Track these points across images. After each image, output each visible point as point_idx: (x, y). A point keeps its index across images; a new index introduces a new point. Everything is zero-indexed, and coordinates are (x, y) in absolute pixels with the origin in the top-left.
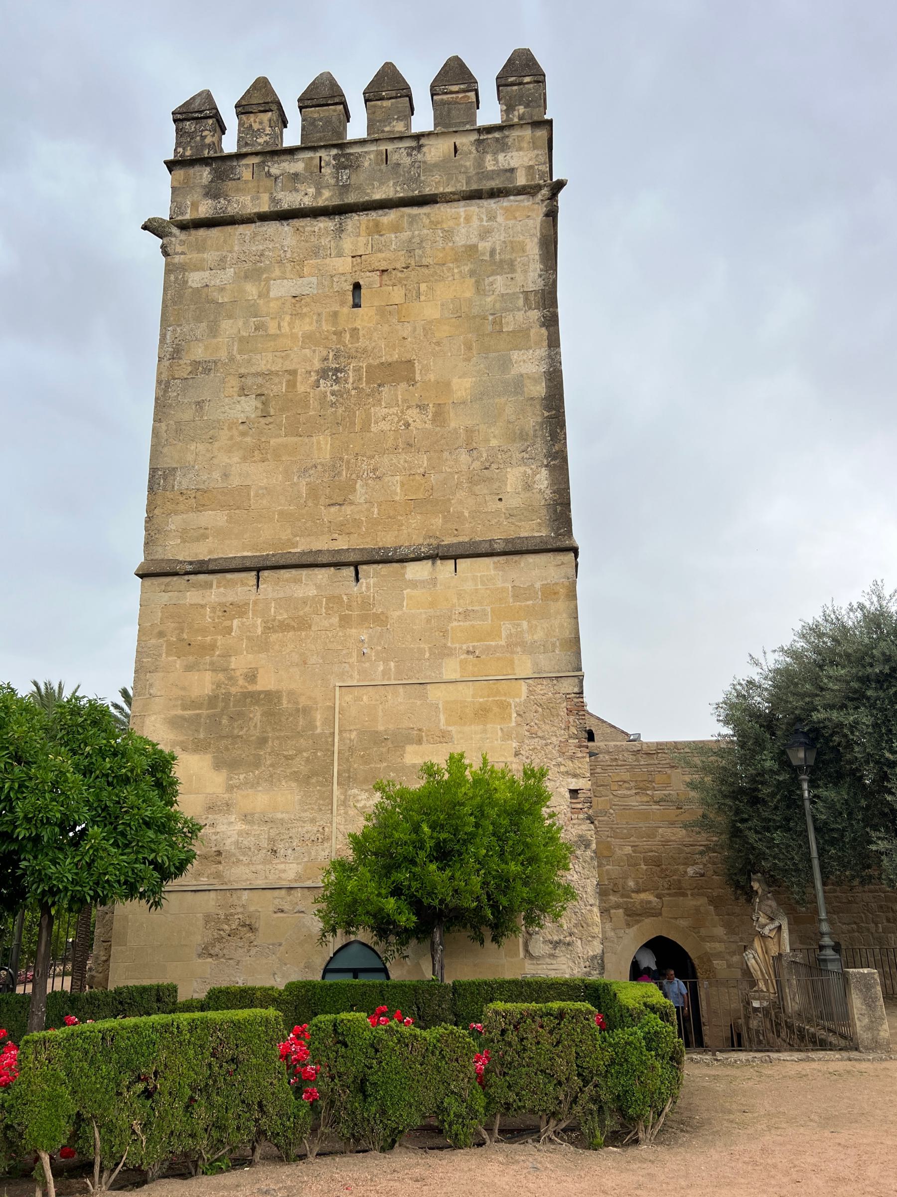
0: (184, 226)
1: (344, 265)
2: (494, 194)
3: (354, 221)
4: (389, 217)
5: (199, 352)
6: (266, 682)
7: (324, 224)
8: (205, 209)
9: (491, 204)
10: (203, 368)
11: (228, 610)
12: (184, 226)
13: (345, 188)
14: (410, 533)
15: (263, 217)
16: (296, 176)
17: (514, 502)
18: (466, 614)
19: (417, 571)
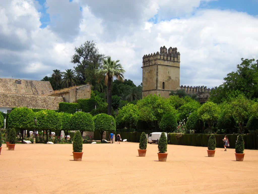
1: (149, 70)
7: (149, 67)
10: (144, 78)
13: (149, 64)
14: (151, 89)
16: (147, 63)
19: (152, 91)
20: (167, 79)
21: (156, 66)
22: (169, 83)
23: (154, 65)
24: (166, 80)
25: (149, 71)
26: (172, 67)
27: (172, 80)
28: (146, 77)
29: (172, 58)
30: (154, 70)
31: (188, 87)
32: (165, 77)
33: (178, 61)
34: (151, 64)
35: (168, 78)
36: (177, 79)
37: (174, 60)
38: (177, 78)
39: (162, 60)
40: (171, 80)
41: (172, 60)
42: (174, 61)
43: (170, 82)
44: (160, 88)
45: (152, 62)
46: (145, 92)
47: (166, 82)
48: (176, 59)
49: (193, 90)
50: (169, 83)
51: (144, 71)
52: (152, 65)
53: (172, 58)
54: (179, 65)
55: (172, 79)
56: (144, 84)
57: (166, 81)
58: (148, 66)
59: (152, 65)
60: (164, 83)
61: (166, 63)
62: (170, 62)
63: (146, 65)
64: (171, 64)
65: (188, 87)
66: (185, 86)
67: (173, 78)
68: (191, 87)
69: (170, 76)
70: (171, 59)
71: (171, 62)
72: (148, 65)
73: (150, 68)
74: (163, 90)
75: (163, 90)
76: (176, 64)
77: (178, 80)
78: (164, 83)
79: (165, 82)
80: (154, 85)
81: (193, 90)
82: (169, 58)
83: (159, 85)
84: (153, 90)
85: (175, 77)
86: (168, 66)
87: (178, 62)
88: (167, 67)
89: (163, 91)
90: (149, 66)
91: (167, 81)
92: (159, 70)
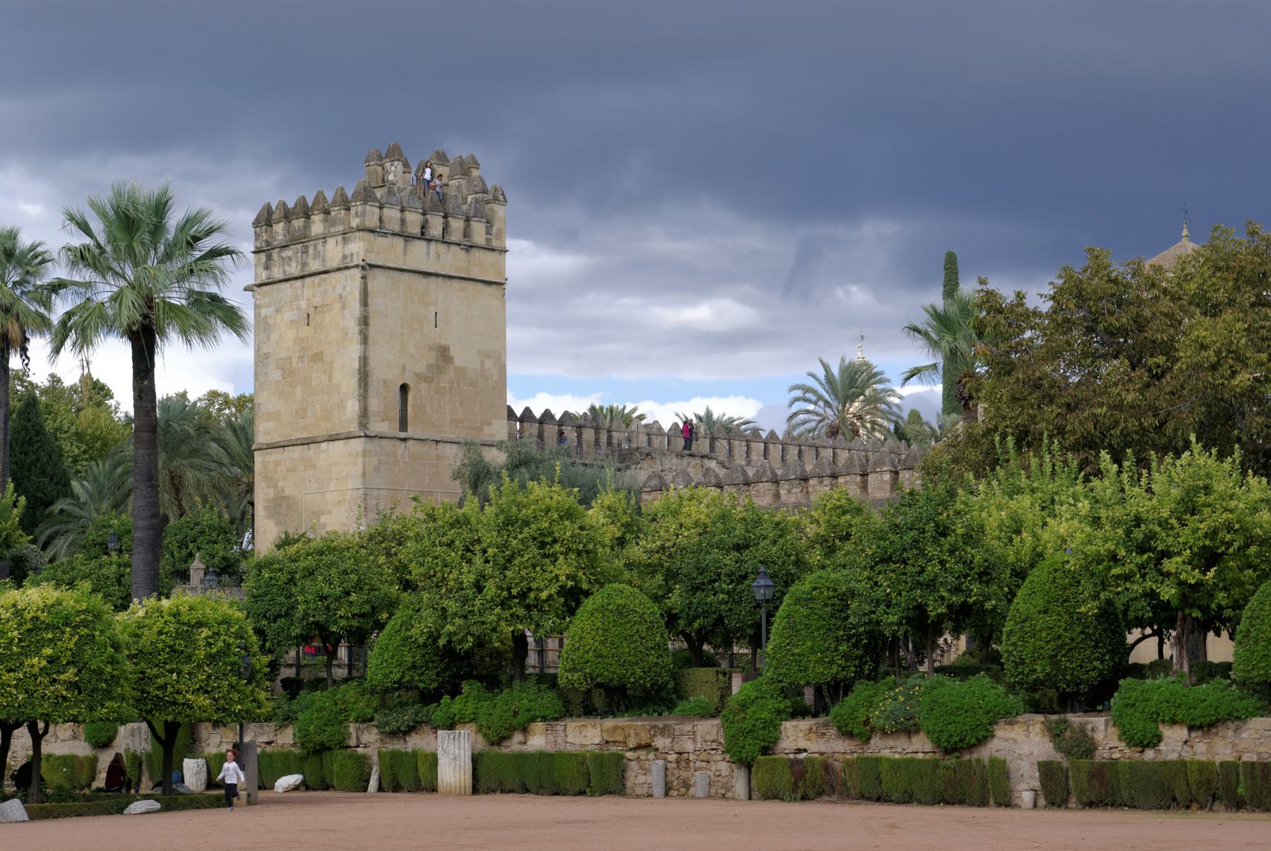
0: (260, 285)
1: (303, 304)
2: (347, 268)
3: (308, 280)
4: (317, 279)
5: (265, 349)
6: (287, 493)
7: (298, 283)
8: (264, 276)
9: (346, 272)
10: (267, 356)
11: (278, 463)
12: (260, 285)
13: (304, 264)
14: (321, 432)
15: (280, 281)
17: (349, 416)
18: (336, 464)
19: (324, 445)
21: (357, 273)
23: (339, 269)
24: (421, 367)
25: (299, 309)
26: (457, 284)
28: (283, 356)
29: (457, 225)
30: (338, 306)
31: (547, 415)
33: (495, 244)
34: (314, 266)
35: (432, 357)
36: (488, 364)
37: (466, 234)
38: (488, 355)
39: (394, 234)
40: (451, 373)
41: (456, 236)
42: (471, 247)
44: (382, 420)
45: (320, 247)
46: (276, 455)
47: (423, 385)
48: (478, 229)
49: (541, 436)
51: (263, 312)
52: (326, 272)
53: (457, 225)
54: (501, 269)
55: (458, 362)
56: (267, 404)
57: (418, 376)
58: (296, 278)
59: (326, 272)
60: (404, 388)
61: (419, 255)
62: (442, 247)
63: (277, 273)
64: (451, 260)
65: (547, 415)
66: (527, 410)
67: (463, 357)
68: (566, 414)
69: (444, 342)
70: (445, 229)
71: (454, 248)
72: (294, 270)
73: (309, 291)
74: (402, 435)
75: (404, 440)
76: (480, 265)
77: (495, 371)
78: (404, 388)
79: (411, 384)
80: (341, 406)
81: (541, 436)
82: (436, 228)
83: (374, 404)
84: (332, 439)
86: (432, 279)
87: (493, 250)
88: (424, 281)
89: (401, 446)
90: (302, 277)
91: (428, 380)
92: (376, 303)
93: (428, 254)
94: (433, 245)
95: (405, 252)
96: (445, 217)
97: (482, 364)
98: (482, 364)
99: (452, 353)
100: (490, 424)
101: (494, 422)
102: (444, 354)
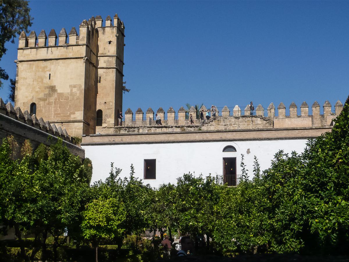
20: (45, 94)
22: (49, 104)
24: (41, 95)
26: (60, 61)
27: (61, 95)
32: (38, 90)
35: (47, 91)
40: (56, 96)
43: (52, 100)
47: (42, 103)
50: (49, 104)
55: (59, 91)
57: (40, 99)
69: (52, 85)
71: (59, 48)
78: (33, 105)
85: (70, 86)
91: (44, 100)
93: (47, 53)
94: (50, 49)
95: (36, 54)
96: (56, 38)
97: (71, 90)
98: (71, 90)
99: (57, 88)
100: (74, 114)
101: (76, 112)
102: (53, 89)
